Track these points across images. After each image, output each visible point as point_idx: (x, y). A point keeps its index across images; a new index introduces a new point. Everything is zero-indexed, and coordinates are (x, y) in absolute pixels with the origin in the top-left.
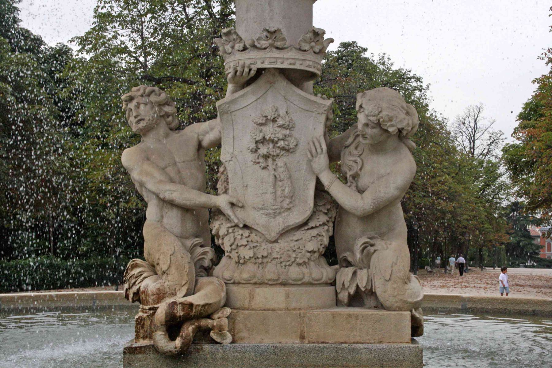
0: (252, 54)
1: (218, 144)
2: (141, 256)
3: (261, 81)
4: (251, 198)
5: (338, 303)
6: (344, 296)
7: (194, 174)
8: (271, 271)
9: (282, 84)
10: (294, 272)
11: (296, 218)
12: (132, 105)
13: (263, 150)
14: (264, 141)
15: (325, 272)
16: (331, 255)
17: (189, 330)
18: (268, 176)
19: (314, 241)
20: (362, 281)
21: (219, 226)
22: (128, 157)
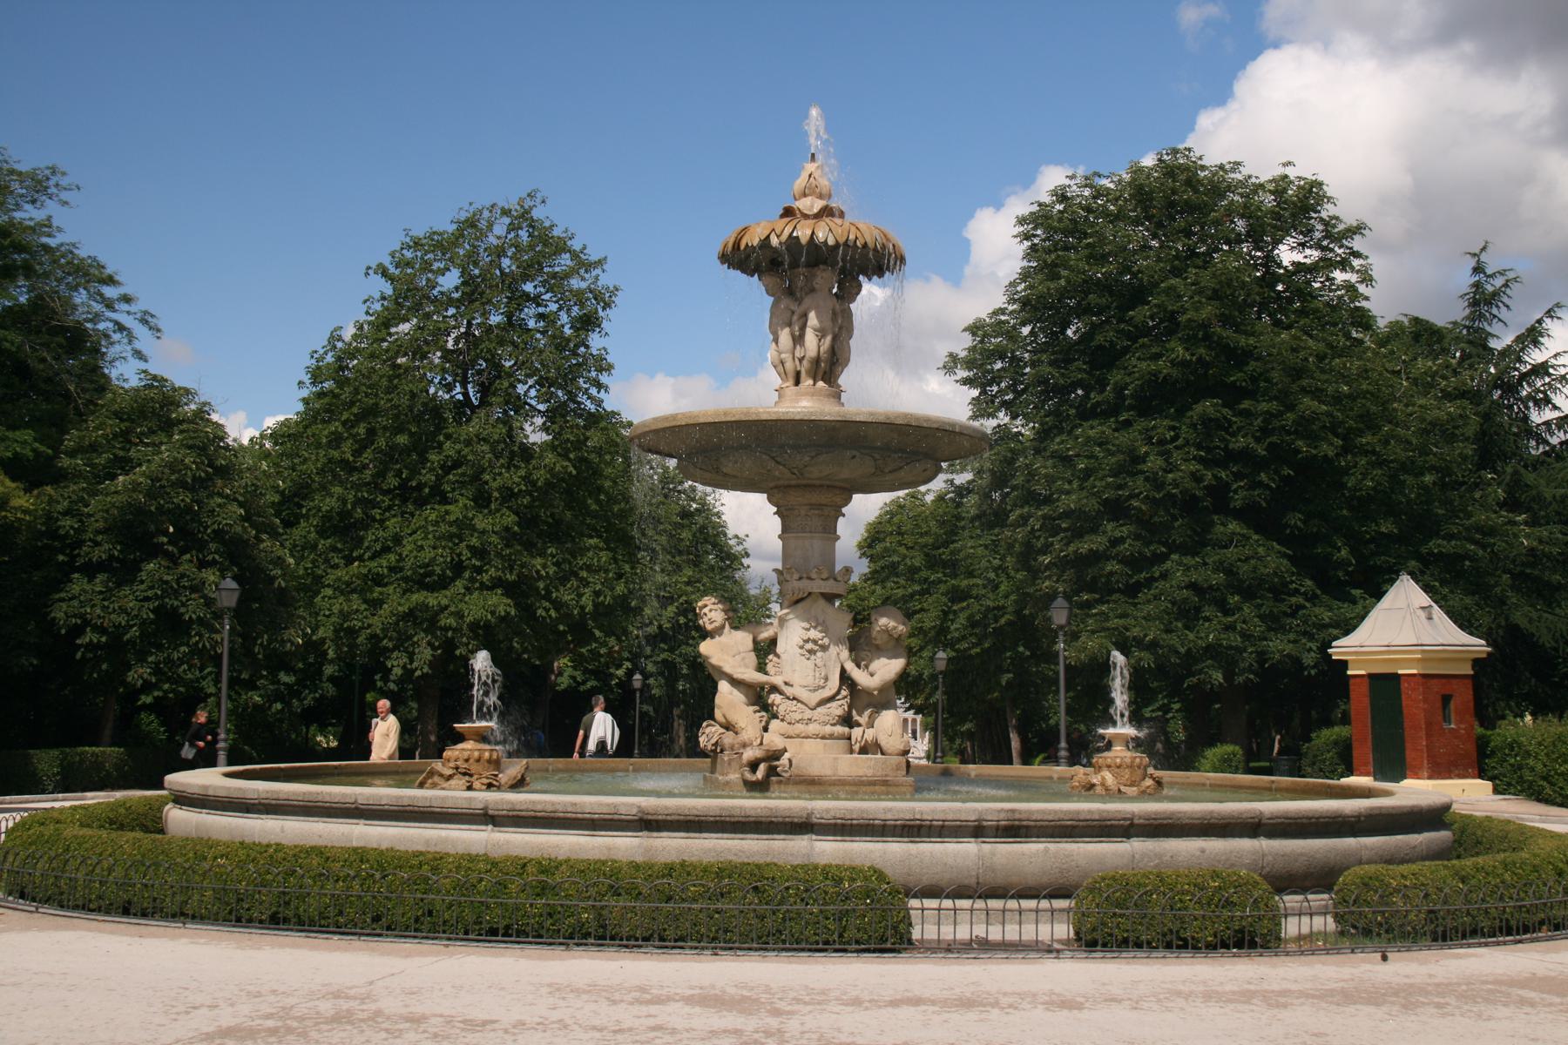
0: (805, 582)
1: (773, 642)
2: (711, 717)
3: (808, 601)
4: (796, 679)
5: (852, 752)
6: (856, 747)
7: (752, 659)
8: (813, 728)
9: (822, 602)
10: (828, 729)
11: (827, 693)
12: (706, 610)
13: (810, 646)
14: (807, 641)
15: (841, 729)
16: (847, 721)
17: (762, 767)
18: (810, 664)
19: (837, 708)
20: (870, 734)
21: (775, 698)
22: (705, 647)
